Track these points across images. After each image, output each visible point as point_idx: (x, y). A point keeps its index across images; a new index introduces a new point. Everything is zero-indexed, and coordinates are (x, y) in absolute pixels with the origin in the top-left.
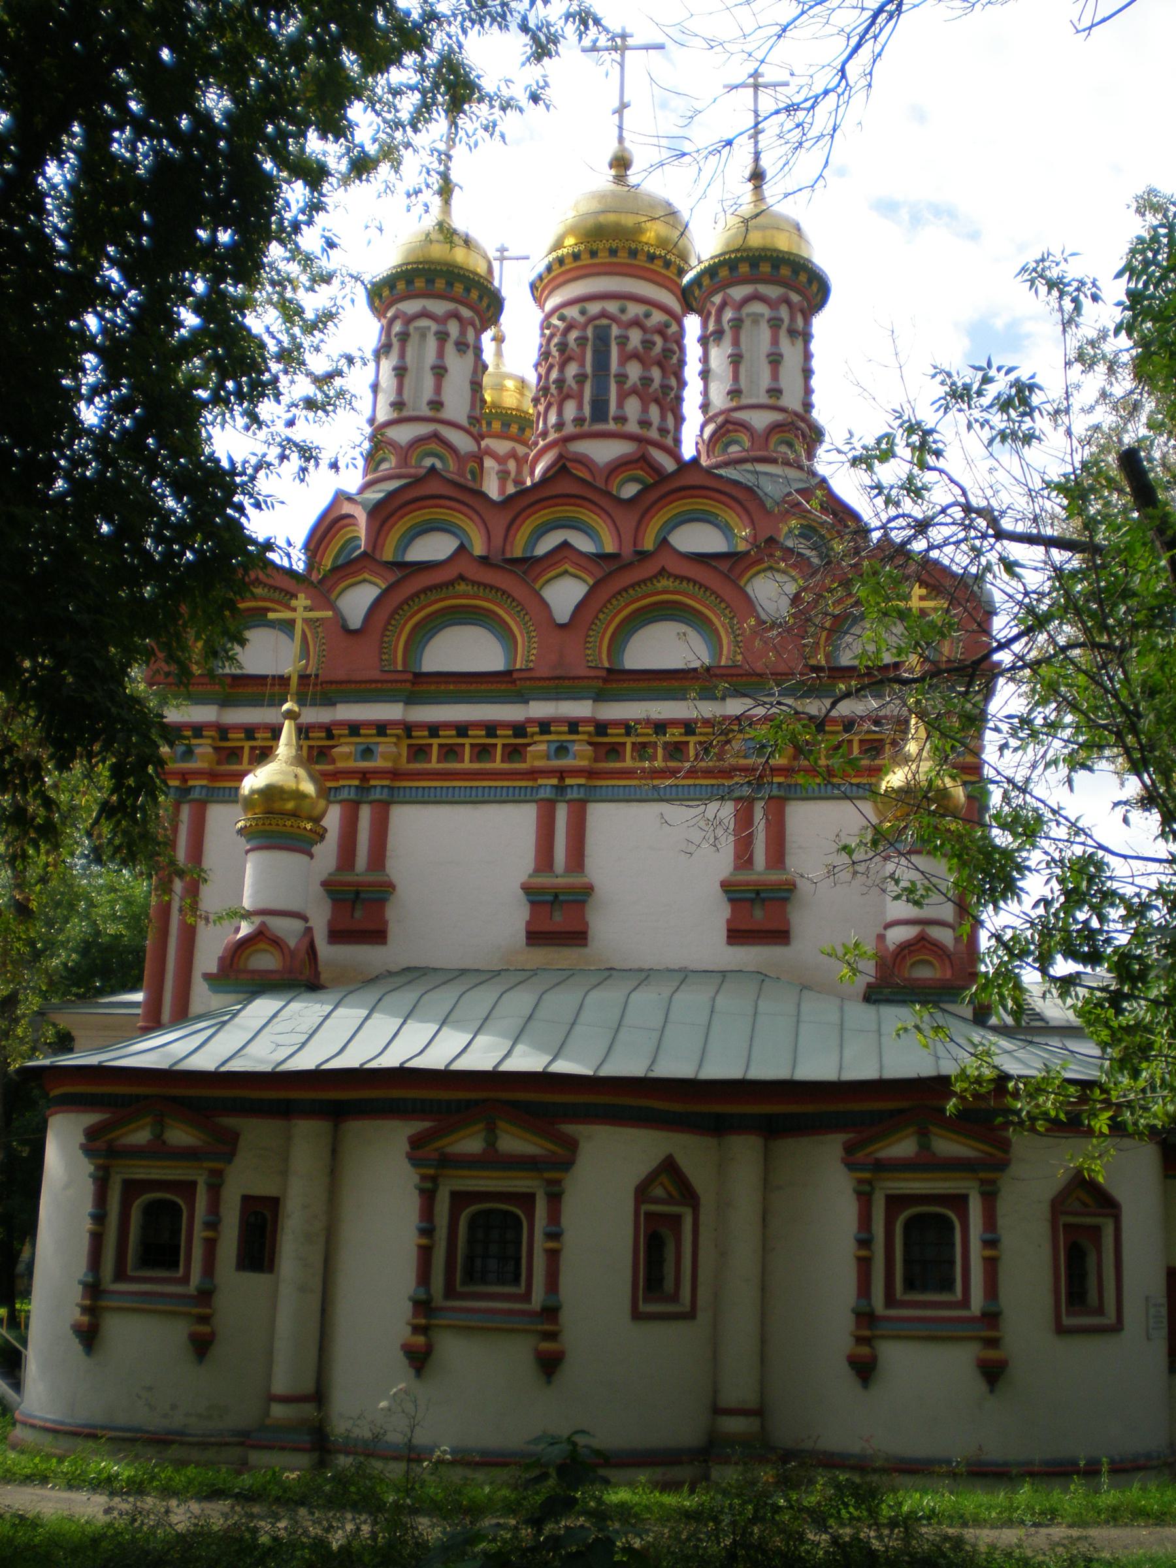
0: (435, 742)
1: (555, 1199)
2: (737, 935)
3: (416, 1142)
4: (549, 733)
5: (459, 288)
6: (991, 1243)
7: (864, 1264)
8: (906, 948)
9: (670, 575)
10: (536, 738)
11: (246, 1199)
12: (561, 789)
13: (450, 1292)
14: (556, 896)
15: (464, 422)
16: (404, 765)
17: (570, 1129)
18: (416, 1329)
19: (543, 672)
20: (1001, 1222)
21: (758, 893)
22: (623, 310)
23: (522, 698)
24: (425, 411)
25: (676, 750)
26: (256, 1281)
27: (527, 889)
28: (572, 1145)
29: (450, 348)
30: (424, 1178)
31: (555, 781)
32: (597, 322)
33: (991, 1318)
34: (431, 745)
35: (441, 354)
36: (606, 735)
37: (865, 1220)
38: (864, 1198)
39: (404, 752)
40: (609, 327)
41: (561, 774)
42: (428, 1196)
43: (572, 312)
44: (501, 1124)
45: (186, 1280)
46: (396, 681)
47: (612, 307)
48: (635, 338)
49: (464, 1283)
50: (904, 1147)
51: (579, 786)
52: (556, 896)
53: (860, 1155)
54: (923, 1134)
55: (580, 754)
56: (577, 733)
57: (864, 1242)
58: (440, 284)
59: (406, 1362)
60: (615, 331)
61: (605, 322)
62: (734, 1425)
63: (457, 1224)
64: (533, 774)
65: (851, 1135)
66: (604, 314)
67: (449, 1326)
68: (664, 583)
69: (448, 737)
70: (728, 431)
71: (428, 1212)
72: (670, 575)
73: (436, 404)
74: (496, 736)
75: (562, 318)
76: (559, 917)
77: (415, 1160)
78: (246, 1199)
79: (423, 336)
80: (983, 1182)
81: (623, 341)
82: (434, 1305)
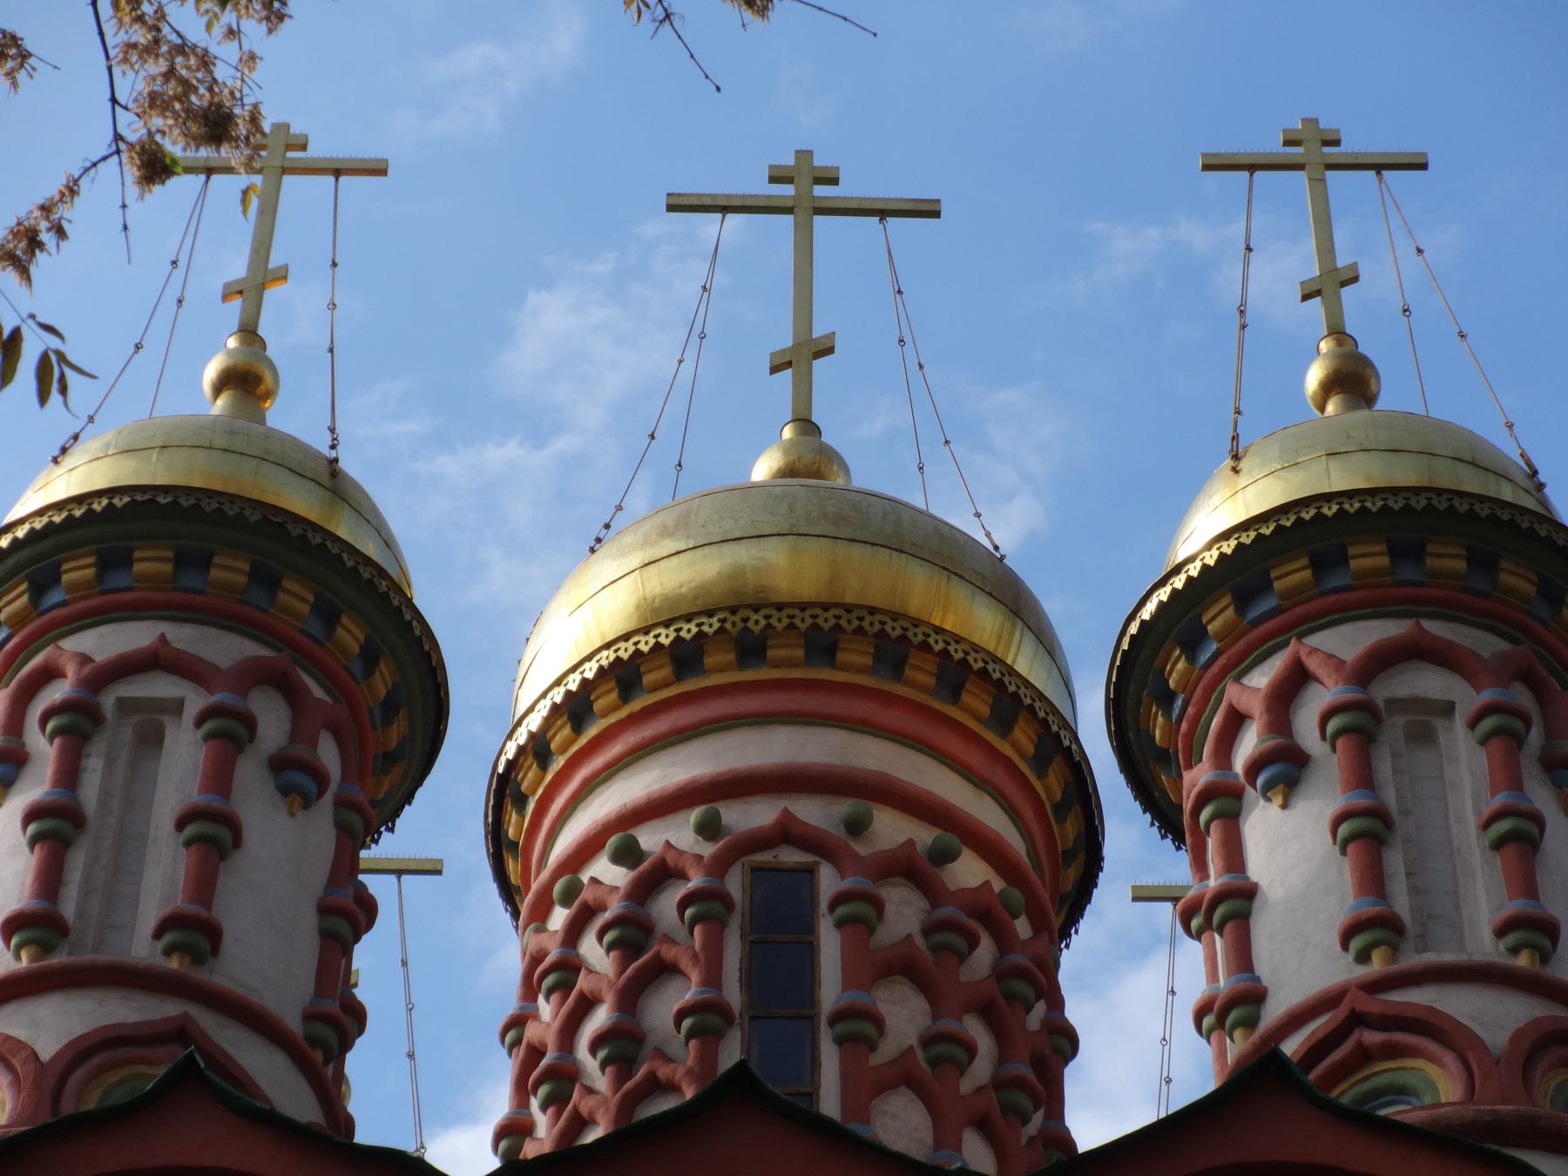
5: (296, 598)
15: (293, 1021)
22: (857, 827)
24: (142, 948)
29: (250, 774)
32: (764, 857)
35: (220, 777)
40: (810, 872)
43: (675, 835)
47: (814, 812)
48: (904, 913)
58: (229, 571)
60: (829, 881)
61: (791, 856)
66: (786, 833)
70: (1364, 1056)
73: (194, 930)
75: (628, 855)
79: (151, 741)
81: (861, 915)
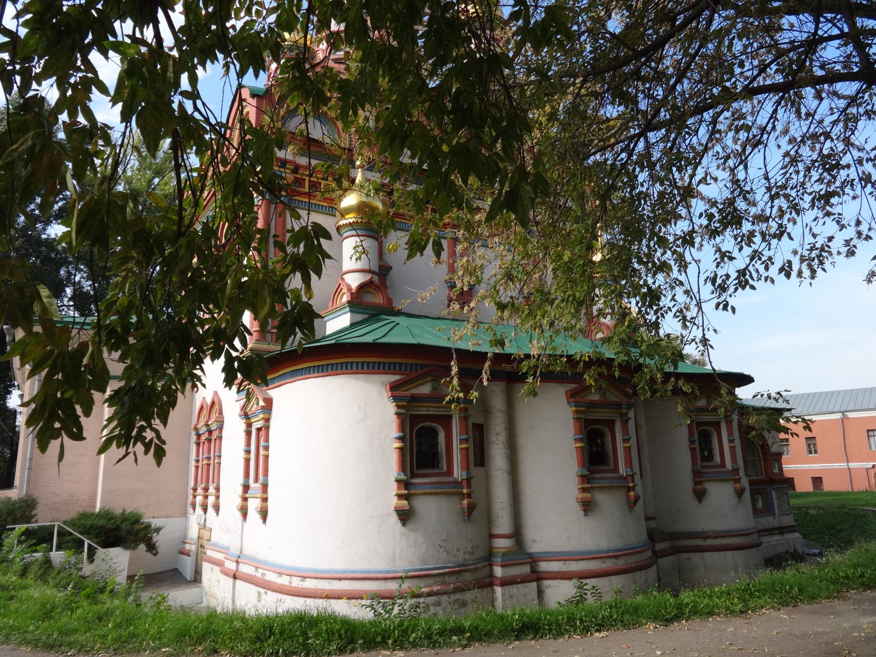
7: (693, 450)
45: (450, 472)
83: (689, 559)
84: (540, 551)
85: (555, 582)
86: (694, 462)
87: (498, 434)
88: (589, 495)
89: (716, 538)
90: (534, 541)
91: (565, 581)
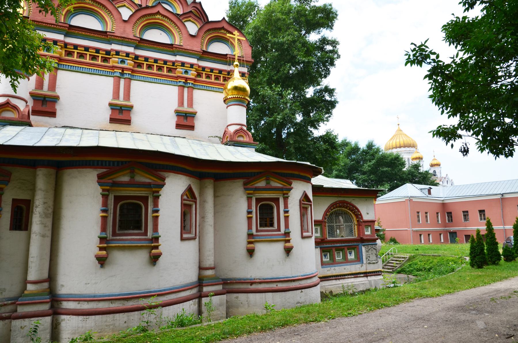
0: (76, 51)
1: (156, 198)
2: (179, 126)
3: (100, 177)
4: (119, 55)
6: (286, 212)
7: (250, 219)
8: (236, 132)
9: (160, 14)
10: (114, 56)
11: (14, 200)
12: (122, 74)
13: (114, 234)
14: (121, 108)
16: (63, 56)
17: (162, 173)
18: (101, 249)
19: (118, 34)
20: (289, 206)
21: (186, 114)
23: (110, 43)
25: (160, 68)
26: (20, 235)
27: (110, 105)
28: (163, 179)
30: (104, 190)
31: (121, 71)
33: (287, 234)
34: (74, 52)
36: (138, 60)
37: (250, 206)
38: (249, 199)
39: (64, 52)
41: (123, 69)
42: (105, 197)
44: (136, 171)
46: (62, 26)
49: (119, 230)
50: (262, 184)
51: (129, 74)
52: (121, 108)
53: (249, 186)
54: (267, 180)
55: (129, 64)
56: (128, 57)
57: (249, 213)
59: (97, 262)
62: (209, 273)
63: (117, 209)
64: (113, 67)
65: (245, 180)
67: (116, 246)
68: (158, 16)
69: (81, 50)
71: (105, 204)
72: (160, 14)
74: (99, 53)
76: (121, 115)
77: (100, 184)
78: (14, 200)
80: (284, 194)
82: (108, 239)
83: (237, 298)
84: (65, 293)
85: (68, 316)
86: (250, 227)
87: (36, 207)
88: (104, 252)
89: (260, 283)
90: (62, 286)
91: (74, 317)
